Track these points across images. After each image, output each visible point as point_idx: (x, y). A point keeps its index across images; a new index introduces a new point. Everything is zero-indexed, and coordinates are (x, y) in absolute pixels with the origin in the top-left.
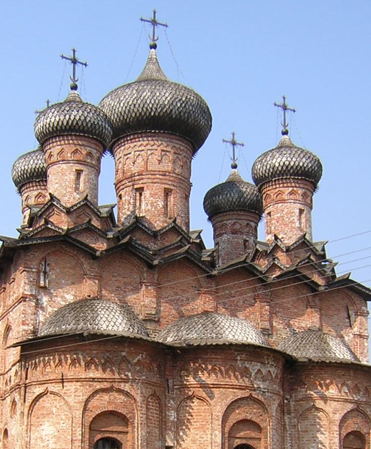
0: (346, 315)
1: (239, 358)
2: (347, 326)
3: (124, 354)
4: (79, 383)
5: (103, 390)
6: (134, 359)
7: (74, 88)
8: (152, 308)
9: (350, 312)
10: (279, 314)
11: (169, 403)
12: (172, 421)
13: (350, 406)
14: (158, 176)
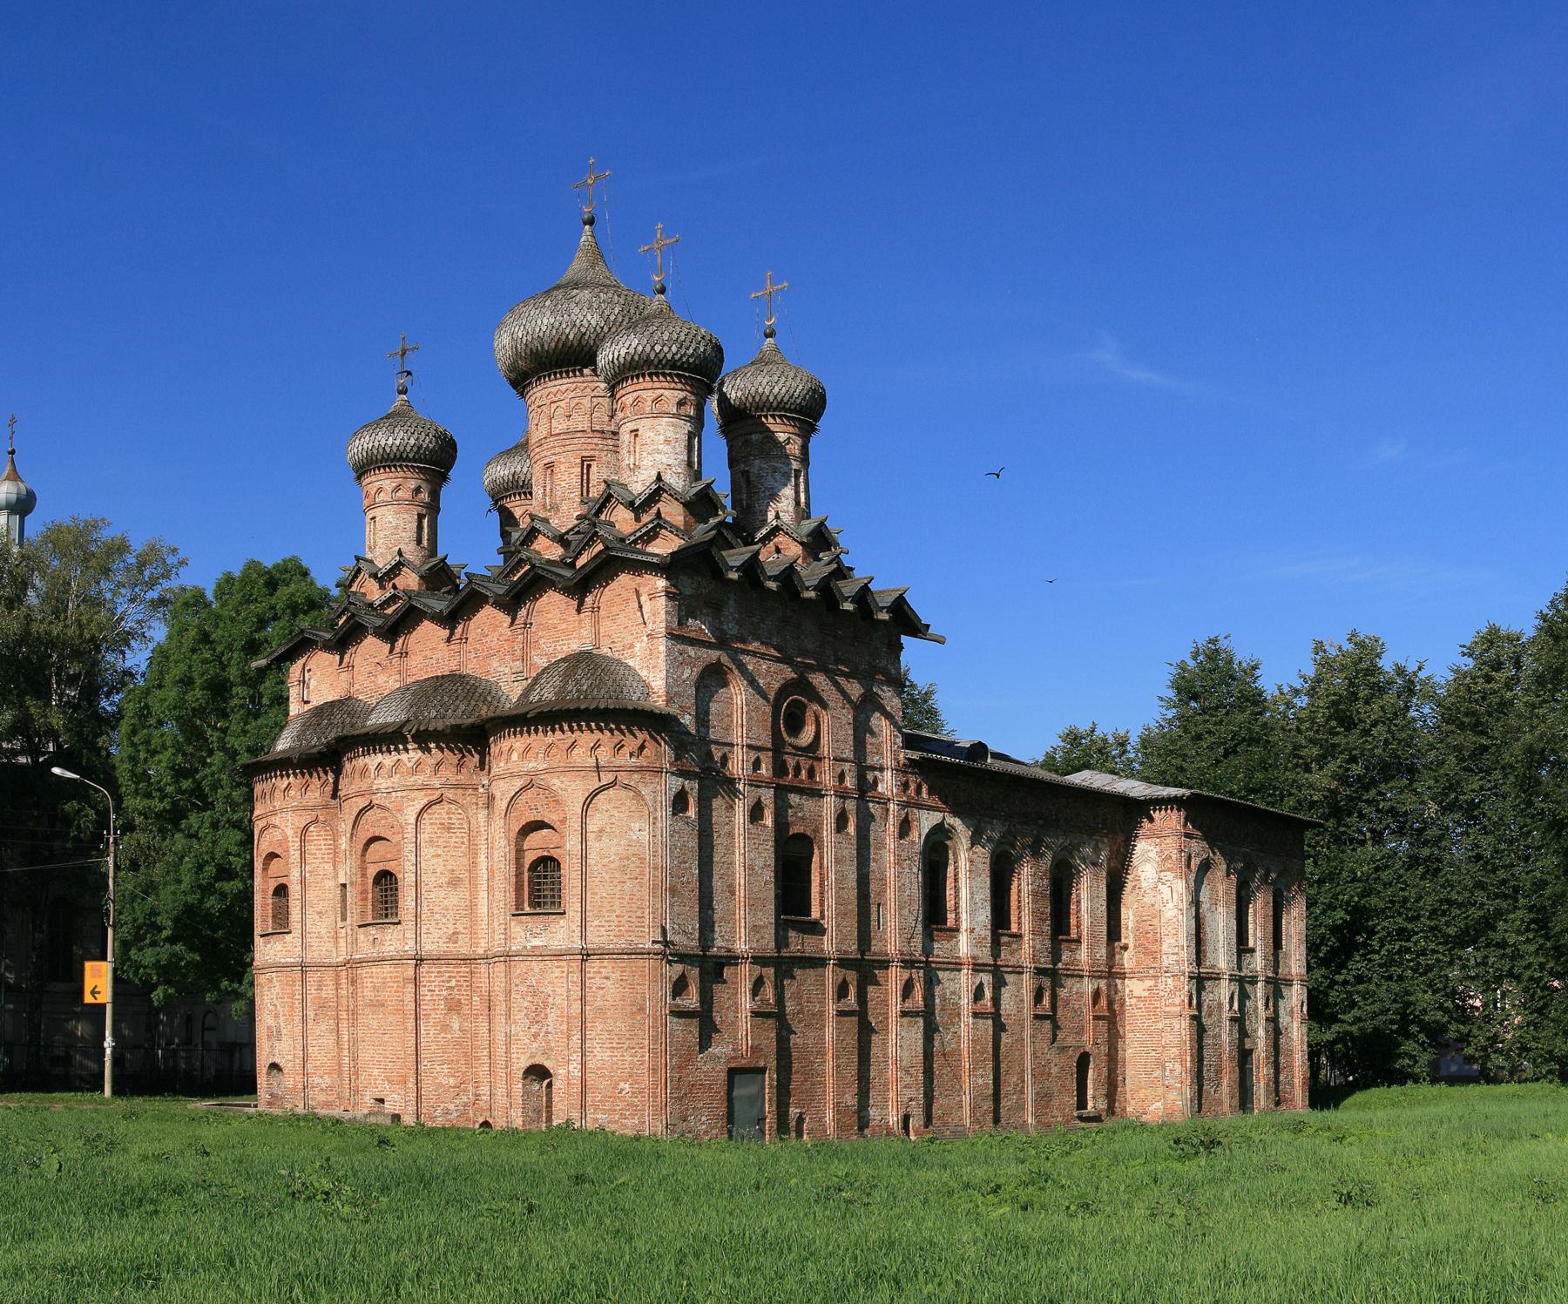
9: (643, 598)
13: (519, 783)
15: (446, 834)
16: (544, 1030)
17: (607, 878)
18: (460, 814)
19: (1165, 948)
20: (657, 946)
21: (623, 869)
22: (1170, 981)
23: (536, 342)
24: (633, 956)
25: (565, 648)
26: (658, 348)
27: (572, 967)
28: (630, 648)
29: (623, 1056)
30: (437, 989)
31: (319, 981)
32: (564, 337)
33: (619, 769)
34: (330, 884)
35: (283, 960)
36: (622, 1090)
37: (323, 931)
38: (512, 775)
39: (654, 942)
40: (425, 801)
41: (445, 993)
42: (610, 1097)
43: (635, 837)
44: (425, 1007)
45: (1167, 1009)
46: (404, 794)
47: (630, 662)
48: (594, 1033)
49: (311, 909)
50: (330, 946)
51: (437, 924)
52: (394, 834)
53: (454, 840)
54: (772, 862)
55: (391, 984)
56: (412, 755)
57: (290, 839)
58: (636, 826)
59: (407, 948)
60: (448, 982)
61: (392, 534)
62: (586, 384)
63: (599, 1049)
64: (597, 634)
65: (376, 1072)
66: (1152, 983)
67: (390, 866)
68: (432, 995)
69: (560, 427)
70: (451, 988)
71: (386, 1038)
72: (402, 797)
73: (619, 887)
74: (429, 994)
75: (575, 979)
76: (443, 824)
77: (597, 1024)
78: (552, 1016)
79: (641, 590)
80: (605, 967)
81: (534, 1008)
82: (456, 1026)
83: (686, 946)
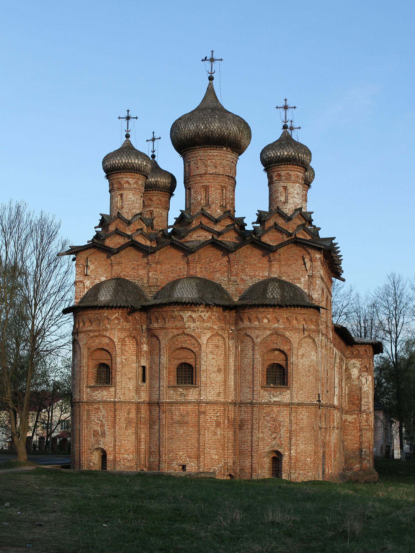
0: (302, 262)
1: (175, 310)
2: (304, 270)
3: (105, 314)
4: (84, 334)
5: (96, 336)
6: (112, 317)
7: (128, 136)
8: (154, 278)
9: (306, 260)
10: (247, 269)
11: (142, 340)
12: (144, 351)
13: (268, 332)
14: (198, 178)
15: (217, 350)
16: (279, 436)
18: (222, 341)
19: (363, 402)
20: (318, 403)
22: (364, 416)
23: (210, 133)
25: (261, 274)
26: (300, 155)
27: (293, 410)
28: (298, 279)
29: (308, 447)
30: (212, 417)
31: (129, 410)
32: (223, 134)
34: (134, 365)
35: (108, 400)
36: (308, 461)
37: (131, 387)
38: (265, 329)
39: (317, 401)
40: (211, 334)
41: (215, 418)
42: (304, 464)
43: (312, 358)
44: (208, 425)
45: (363, 427)
46: (202, 330)
47: (299, 285)
48: (299, 438)
49: (125, 377)
50: (133, 394)
51: (213, 388)
52: (195, 347)
53: (219, 352)
55: (191, 414)
56: (206, 315)
57: (116, 343)
59: (202, 398)
60: (217, 413)
61: (132, 204)
62: (224, 154)
63: (301, 444)
64: (280, 271)
65: (181, 453)
66: (356, 416)
67: (191, 361)
68: (210, 419)
69: (212, 171)
70: (217, 416)
71: (188, 438)
72: (200, 332)
74: (209, 419)
75: (294, 415)
76: (216, 345)
77: (301, 434)
78: (283, 430)
79: (305, 256)
80: (303, 411)
81: (274, 427)
82: (219, 433)
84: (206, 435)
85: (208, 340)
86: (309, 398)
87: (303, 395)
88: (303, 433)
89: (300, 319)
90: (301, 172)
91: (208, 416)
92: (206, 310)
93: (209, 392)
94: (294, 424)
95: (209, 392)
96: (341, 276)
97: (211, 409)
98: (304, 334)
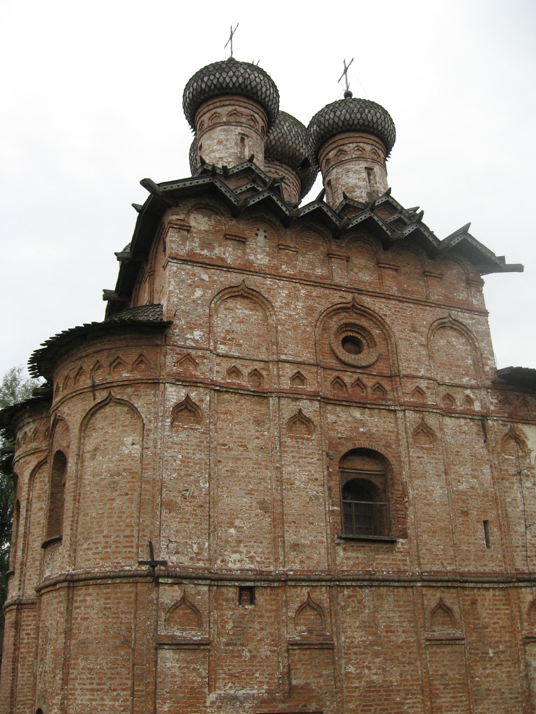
17: (98, 497)
20: (144, 568)
21: (113, 486)
24: (118, 581)
33: (108, 386)
39: (141, 563)
44: (22, 650)
48: (76, 672)
54: (320, 475)
58: (128, 440)
63: (79, 691)
68: (28, 639)
73: (108, 506)
74: (26, 637)
77: (79, 661)
80: (90, 594)
83: (184, 568)
84: (19, 675)
85: (33, 474)
86: (109, 558)
87: (90, 552)
88: (87, 659)
89: (88, 366)
90: (224, 106)
91: (24, 632)
92: (31, 420)
93: (29, 580)
94: (61, 633)
95: (29, 580)
96: (507, 262)
97: (30, 616)
98: (94, 399)
